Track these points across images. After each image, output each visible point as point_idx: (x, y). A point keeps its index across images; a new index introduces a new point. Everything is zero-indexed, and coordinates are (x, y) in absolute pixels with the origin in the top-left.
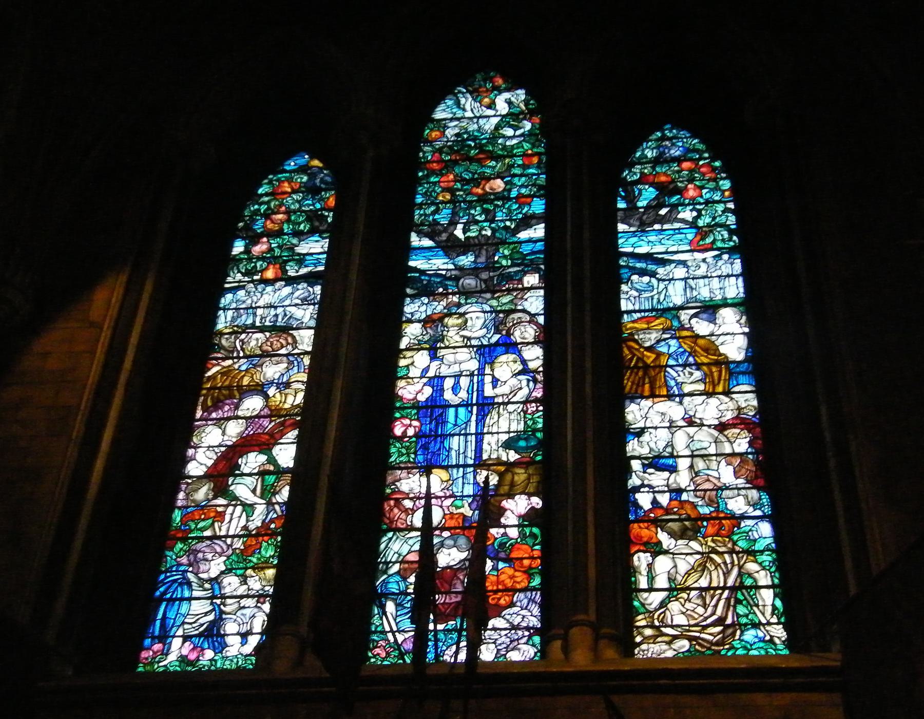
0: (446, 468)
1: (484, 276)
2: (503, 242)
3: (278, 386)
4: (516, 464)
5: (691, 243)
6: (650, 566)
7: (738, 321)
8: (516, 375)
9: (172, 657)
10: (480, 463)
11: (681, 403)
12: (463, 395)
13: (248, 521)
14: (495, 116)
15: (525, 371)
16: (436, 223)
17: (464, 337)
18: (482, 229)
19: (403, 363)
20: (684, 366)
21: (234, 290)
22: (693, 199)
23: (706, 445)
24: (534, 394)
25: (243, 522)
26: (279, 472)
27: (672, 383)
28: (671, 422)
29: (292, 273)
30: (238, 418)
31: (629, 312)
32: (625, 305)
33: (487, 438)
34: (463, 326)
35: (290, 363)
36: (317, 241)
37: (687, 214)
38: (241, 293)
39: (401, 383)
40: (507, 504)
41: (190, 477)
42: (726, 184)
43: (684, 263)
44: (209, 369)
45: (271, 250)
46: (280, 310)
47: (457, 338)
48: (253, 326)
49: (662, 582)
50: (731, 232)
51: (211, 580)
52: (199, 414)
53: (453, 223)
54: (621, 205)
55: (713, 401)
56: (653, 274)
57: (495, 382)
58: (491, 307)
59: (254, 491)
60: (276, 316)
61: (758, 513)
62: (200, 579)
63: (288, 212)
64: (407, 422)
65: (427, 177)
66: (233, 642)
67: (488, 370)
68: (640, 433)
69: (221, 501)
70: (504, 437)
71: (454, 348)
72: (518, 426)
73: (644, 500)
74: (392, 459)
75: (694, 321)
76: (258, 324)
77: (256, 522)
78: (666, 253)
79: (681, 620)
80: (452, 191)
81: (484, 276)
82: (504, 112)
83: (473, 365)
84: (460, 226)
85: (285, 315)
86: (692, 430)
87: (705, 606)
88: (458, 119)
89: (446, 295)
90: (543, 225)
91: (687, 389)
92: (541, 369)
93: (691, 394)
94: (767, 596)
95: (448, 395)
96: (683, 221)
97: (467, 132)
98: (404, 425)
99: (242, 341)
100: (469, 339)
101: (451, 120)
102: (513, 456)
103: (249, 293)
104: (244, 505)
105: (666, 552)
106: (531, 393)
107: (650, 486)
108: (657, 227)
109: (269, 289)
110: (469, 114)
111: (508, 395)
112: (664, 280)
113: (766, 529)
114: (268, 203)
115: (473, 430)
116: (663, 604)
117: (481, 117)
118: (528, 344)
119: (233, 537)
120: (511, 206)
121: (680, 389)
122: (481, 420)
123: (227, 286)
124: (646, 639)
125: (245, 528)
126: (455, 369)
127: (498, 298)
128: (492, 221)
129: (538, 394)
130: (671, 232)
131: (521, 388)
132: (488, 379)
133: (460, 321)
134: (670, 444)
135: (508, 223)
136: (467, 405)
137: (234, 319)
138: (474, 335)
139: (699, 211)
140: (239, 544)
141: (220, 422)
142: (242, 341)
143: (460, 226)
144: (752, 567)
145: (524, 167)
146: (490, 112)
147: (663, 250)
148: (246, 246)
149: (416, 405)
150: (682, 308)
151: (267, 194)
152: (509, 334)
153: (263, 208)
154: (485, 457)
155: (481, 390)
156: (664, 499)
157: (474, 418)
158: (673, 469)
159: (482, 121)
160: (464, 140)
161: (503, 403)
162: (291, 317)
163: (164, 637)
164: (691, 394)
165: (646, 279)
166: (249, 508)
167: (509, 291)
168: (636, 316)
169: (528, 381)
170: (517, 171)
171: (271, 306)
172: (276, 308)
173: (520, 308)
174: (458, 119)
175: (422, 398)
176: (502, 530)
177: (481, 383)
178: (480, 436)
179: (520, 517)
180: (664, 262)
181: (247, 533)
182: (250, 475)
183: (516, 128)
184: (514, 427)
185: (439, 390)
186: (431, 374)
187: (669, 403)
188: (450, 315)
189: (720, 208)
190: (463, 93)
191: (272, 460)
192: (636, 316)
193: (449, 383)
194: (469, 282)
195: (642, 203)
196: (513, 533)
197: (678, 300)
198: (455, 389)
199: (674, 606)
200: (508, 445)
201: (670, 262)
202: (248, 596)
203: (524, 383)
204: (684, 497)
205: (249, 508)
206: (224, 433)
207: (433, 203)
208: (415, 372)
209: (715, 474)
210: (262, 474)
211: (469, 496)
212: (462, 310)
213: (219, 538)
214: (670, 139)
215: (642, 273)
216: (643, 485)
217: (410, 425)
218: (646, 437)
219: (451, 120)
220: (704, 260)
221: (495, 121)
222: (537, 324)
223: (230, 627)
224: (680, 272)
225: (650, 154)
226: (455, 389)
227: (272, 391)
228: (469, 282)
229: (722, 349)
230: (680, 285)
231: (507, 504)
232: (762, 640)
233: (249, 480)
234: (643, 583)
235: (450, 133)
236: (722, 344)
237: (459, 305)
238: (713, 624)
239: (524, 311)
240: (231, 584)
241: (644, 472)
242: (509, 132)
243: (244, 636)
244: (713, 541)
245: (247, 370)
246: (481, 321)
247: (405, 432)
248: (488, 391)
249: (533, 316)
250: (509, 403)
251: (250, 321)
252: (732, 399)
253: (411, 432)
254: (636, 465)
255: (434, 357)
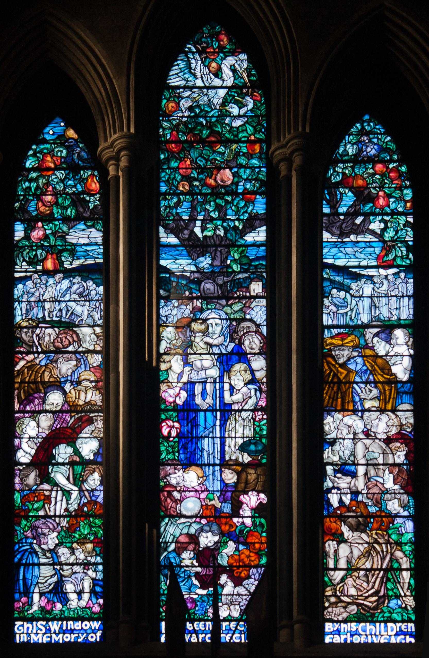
0: (201, 466)
1: (220, 280)
2: (234, 245)
3: (72, 382)
4: (249, 465)
5: (378, 258)
6: (336, 551)
7: (406, 343)
8: (246, 384)
9: (35, 608)
10: (224, 464)
11: (362, 417)
12: (209, 400)
13: (68, 504)
14: (221, 87)
15: (253, 381)
16: (178, 218)
17: (206, 343)
18: (216, 228)
19: (163, 367)
20: (367, 382)
21: (23, 280)
22: (382, 208)
23: (376, 455)
24: (260, 403)
25: (64, 506)
26: (85, 463)
27: (357, 399)
28: (355, 434)
29: (67, 265)
30: (46, 411)
31: (330, 327)
32: (327, 320)
33: (228, 441)
34: (205, 332)
35: (78, 360)
36: (83, 230)
37: (376, 226)
38: (29, 284)
39: (163, 387)
40: (244, 498)
41: (21, 464)
42: (408, 194)
43: (370, 278)
44: (17, 363)
45: (46, 237)
46: (63, 305)
47: (202, 345)
48: (43, 320)
49: (342, 564)
50: (409, 248)
51: (50, 550)
52: (17, 407)
53: (193, 219)
54: (326, 210)
55: (384, 418)
56: (347, 289)
57: (232, 388)
58: (226, 314)
59: (68, 479)
60: (60, 310)
61: (406, 514)
62: (42, 549)
63: (56, 194)
64: (170, 423)
65: (168, 160)
66: (73, 596)
67: (226, 379)
68: (333, 443)
69: (46, 486)
70: (240, 441)
71: (200, 354)
72: (249, 432)
73: (334, 499)
74: (163, 456)
75: (376, 339)
76: (47, 319)
77: (74, 507)
78: (359, 267)
79: (353, 592)
80: (188, 179)
81: (220, 280)
82: (230, 83)
83: (214, 372)
84: (198, 223)
85: (68, 311)
86: (368, 442)
87: (368, 582)
88: (191, 88)
89: (191, 299)
90: (264, 228)
91: (368, 405)
92: (265, 380)
93: (369, 410)
94: (406, 575)
95: (198, 400)
96: (373, 233)
97: (198, 106)
98: (169, 426)
99: (38, 335)
100: (211, 346)
101: (185, 88)
102: (247, 459)
103: (36, 284)
104: (63, 491)
105: (345, 541)
106: (257, 402)
107: (339, 489)
108: (353, 237)
109: (51, 281)
110: (199, 83)
111: (241, 403)
112: (356, 297)
113: (410, 525)
114: (36, 180)
115: (218, 435)
116: (343, 580)
117: (208, 88)
118: (255, 354)
119: (60, 516)
120: (238, 203)
121: (362, 405)
122: (223, 426)
123: (17, 275)
124: (331, 604)
125: (67, 510)
126: (202, 374)
127: (231, 306)
128: (224, 220)
129: (263, 403)
130: (363, 245)
131: (250, 397)
132: (227, 387)
133: (203, 327)
134: (353, 454)
135: (237, 223)
136: (212, 410)
137: (28, 312)
138: (215, 342)
139: (386, 222)
140: (64, 523)
141: (34, 414)
142: (38, 335)
143: (198, 223)
144: (399, 554)
145: (249, 156)
146: (217, 82)
147: (356, 264)
148: (25, 230)
149: (176, 408)
150: (368, 326)
151: (34, 169)
152: (241, 344)
153: (34, 185)
154: (227, 458)
155: (222, 397)
156: (347, 499)
157: (218, 423)
158: (354, 475)
159: (211, 93)
160: (197, 116)
161: (240, 411)
162: (72, 313)
163: (27, 593)
164: (369, 410)
165: (342, 294)
166: (67, 493)
167: (240, 298)
168: (334, 331)
169: (256, 390)
170: (242, 161)
171: (55, 300)
172: (59, 302)
173: (248, 317)
174: (191, 88)
175: (180, 401)
176: (241, 520)
177: (222, 389)
178: (223, 439)
179: (252, 509)
180: (357, 277)
181: (68, 514)
182: (63, 464)
183: (241, 105)
184: (246, 433)
185: (192, 396)
186: (185, 379)
187: (354, 417)
188: (195, 320)
189: (402, 220)
190: (193, 53)
191: (77, 452)
192: (334, 331)
193: (198, 388)
194: (208, 286)
195: (343, 209)
196: (248, 521)
197: (365, 319)
198: (204, 394)
199: (349, 581)
200: (243, 448)
201: (363, 276)
202: (77, 564)
203: (253, 392)
204: (360, 498)
205: (67, 493)
206: (38, 426)
207: (175, 194)
208: (173, 377)
209: (381, 480)
210: (72, 464)
211: (218, 491)
212: (204, 316)
213: (50, 517)
214: (368, 134)
215: (341, 287)
216: (334, 488)
217: (173, 427)
218: (337, 447)
219: (185, 88)
220: (386, 277)
221: (222, 93)
222: (261, 334)
223: (69, 587)
224: (368, 290)
225: (351, 150)
226: (204, 394)
227: (68, 387)
228: (208, 286)
229: (394, 369)
230: (367, 302)
231: (244, 498)
232: (400, 607)
233: (64, 469)
234: (331, 565)
235: (184, 104)
236: (394, 364)
237: (201, 310)
238: (372, 595)
239: (251, 320)
240: (63, 551)
241: (335, 476)
242: (235, 110)
243: (80, 594)
244: (376, 534)
245: (46, 365)
246: (219, 329)
247: (170, 433)
248: (227, 398)
249: (258, 326)
250: (243, 410)
251: (40, 316)
252: (397, 416)
253: (174, 433)
254: (329, 469)
255: (186, 363)
